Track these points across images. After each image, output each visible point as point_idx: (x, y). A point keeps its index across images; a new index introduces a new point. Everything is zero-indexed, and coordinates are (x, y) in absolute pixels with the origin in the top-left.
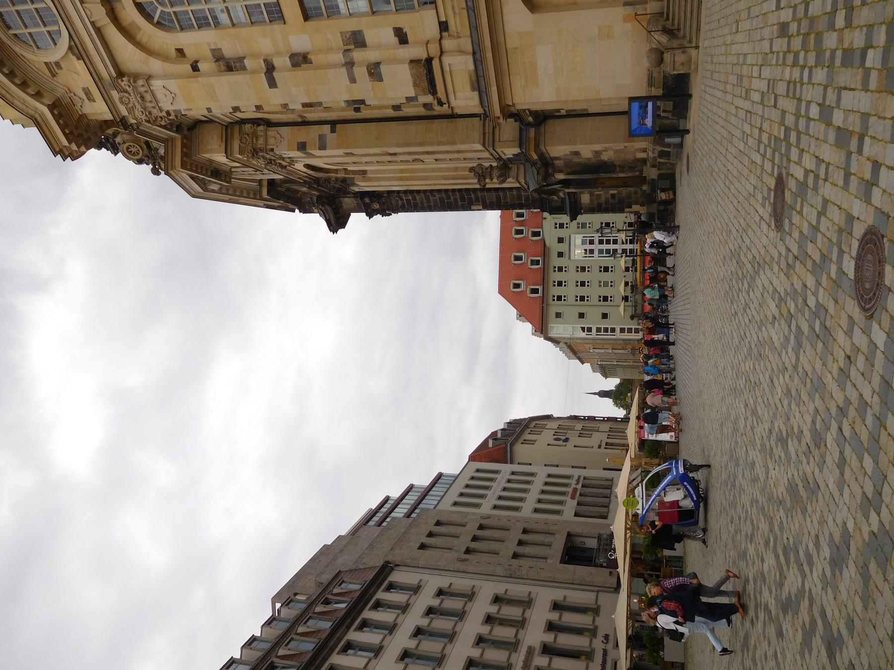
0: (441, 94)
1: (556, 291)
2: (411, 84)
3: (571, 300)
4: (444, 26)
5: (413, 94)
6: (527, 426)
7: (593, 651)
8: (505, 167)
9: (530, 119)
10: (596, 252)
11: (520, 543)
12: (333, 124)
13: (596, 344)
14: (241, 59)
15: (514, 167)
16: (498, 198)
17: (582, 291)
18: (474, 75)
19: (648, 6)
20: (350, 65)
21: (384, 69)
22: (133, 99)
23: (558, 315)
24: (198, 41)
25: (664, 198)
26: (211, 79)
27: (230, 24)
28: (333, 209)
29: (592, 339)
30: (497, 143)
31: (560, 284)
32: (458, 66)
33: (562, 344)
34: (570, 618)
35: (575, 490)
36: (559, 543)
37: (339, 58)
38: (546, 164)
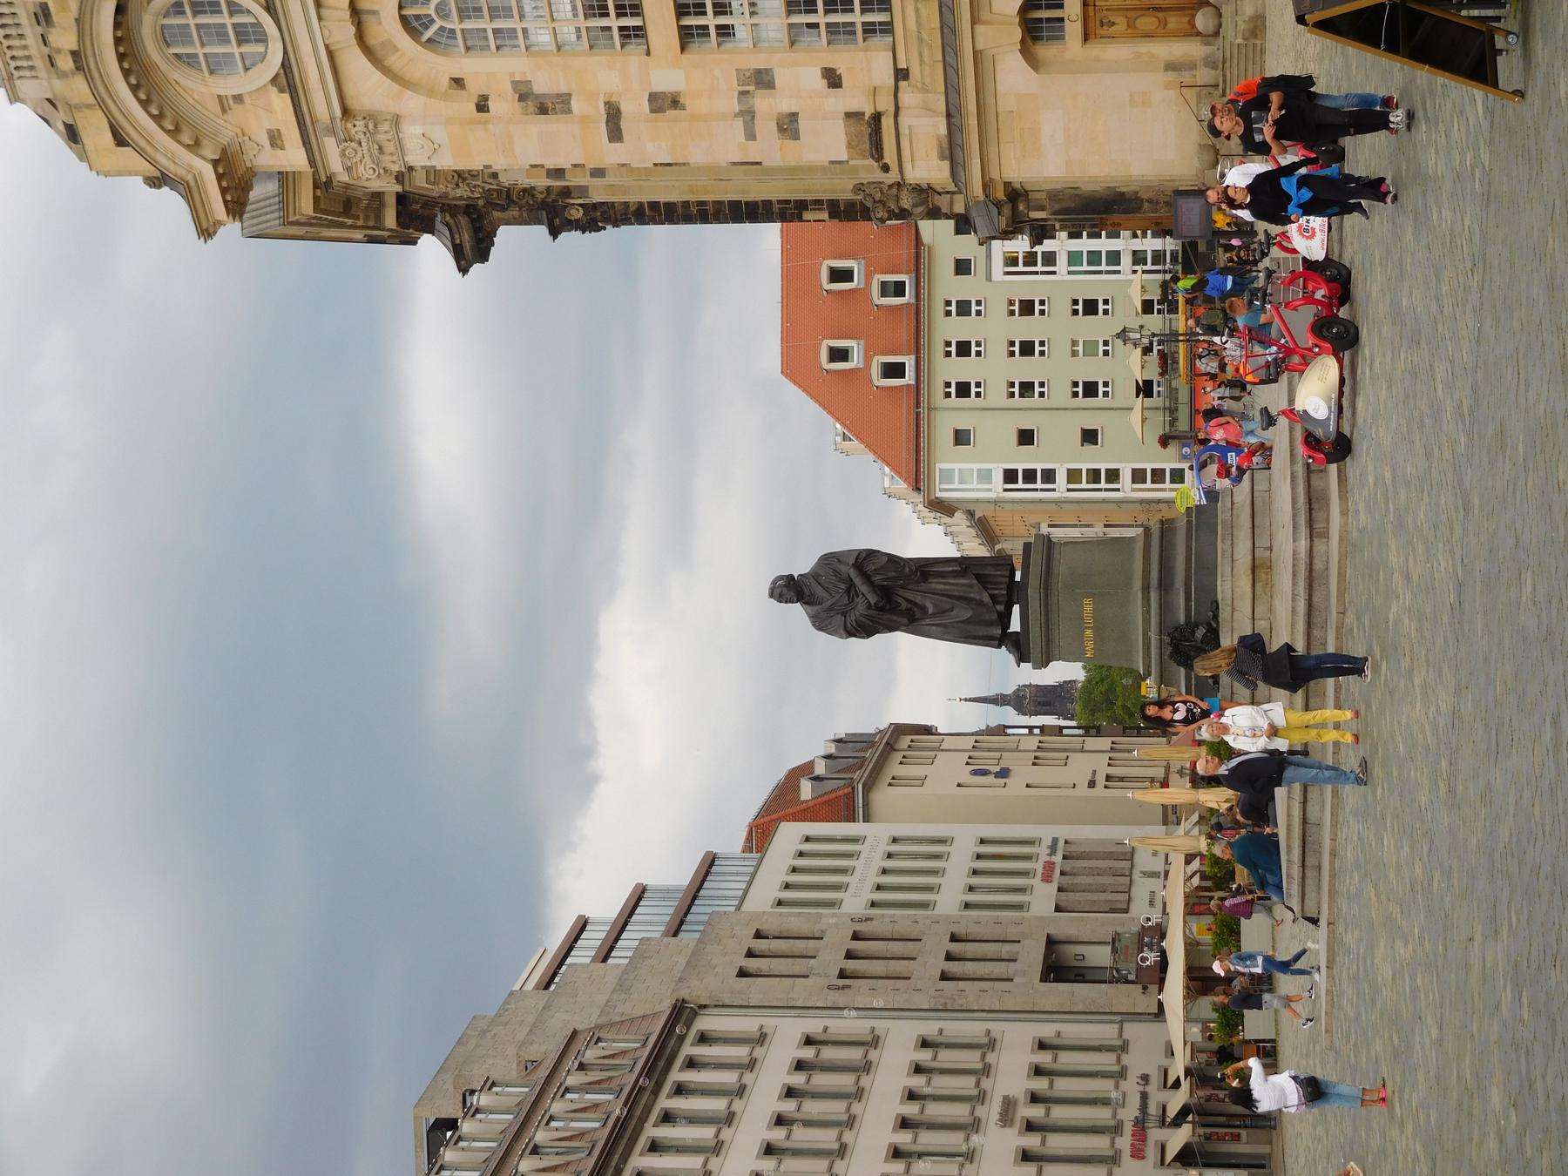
0: (890, 156)
1: (955, 369)
3: (996, 393)
4: (901, 74)
5: (845, 158)
6: (890, 747)
11: (949, 957)
17: (1026, 369)
19: (1197, 73)
20: (748, 115)
21: (803, 124)
23: (961, 438)
24: (491, 70)
28: (473, 221)
29: (1057, 502)
31: (964, 349)
33: (959, 516)
35: (1049, 866)
36: (1033, 955)
37: (734, 105)
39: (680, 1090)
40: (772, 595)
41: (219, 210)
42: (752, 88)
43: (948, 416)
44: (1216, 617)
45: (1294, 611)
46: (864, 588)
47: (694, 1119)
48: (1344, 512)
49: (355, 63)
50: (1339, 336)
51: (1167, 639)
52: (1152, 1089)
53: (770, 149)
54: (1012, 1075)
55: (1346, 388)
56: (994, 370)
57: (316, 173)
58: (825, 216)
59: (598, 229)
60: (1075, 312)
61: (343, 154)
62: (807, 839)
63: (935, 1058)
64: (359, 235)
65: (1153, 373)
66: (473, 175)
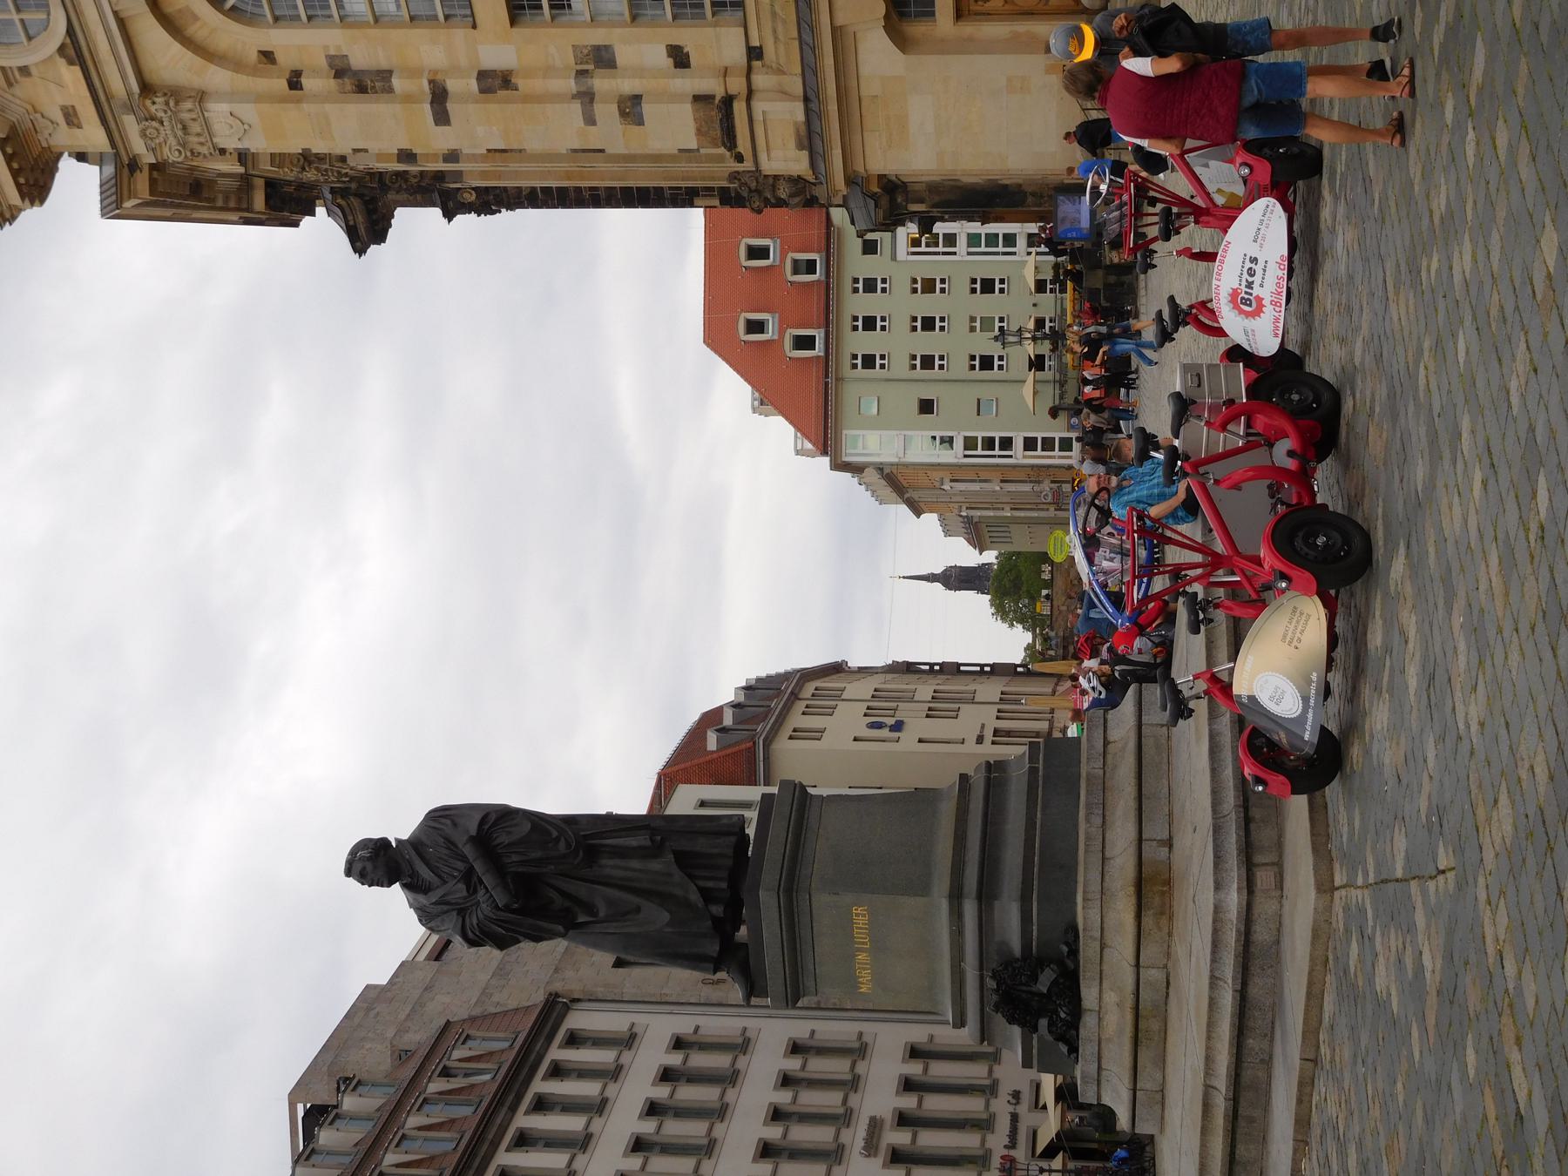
0: (743, 145)
1: (862, 343)
4: (754, 53)
5: (694, 145)
6: (795, 696)
7: (992, 1117)
10: (962, 242)
13: (955, 472)
18: (803, 129)
20: (587, 98)
21: (647, 108)
24: (304, 44)
25: (1116, 260)
26: (328, 107)
27: (371, 19)
28: (366, 203)
31: (869, 324)
33: (870, 474)
37: (570, 85)
39: (557, 1071)
40: (348, 873)
41: (13, 196)
42: (591, 67)
44: (1074, 953)
45: (1214, 980)
46: (488, 880)
47: (584, 1073)
48: (1326, 887)
49: (152, 35)
50: (1332, 555)
51: (991, 984)
52: (1023, 1109)
53: (610, 133)
54: (880, 1097)
55: (1347, 656)
56: (898, 343)
57: (117, 155)
58: (716, 202)
59: (493, 213)
60: (973, 291)
61: (143, 134)
63: (804, 1067)
64: (235, 217)
66: (320, 158)
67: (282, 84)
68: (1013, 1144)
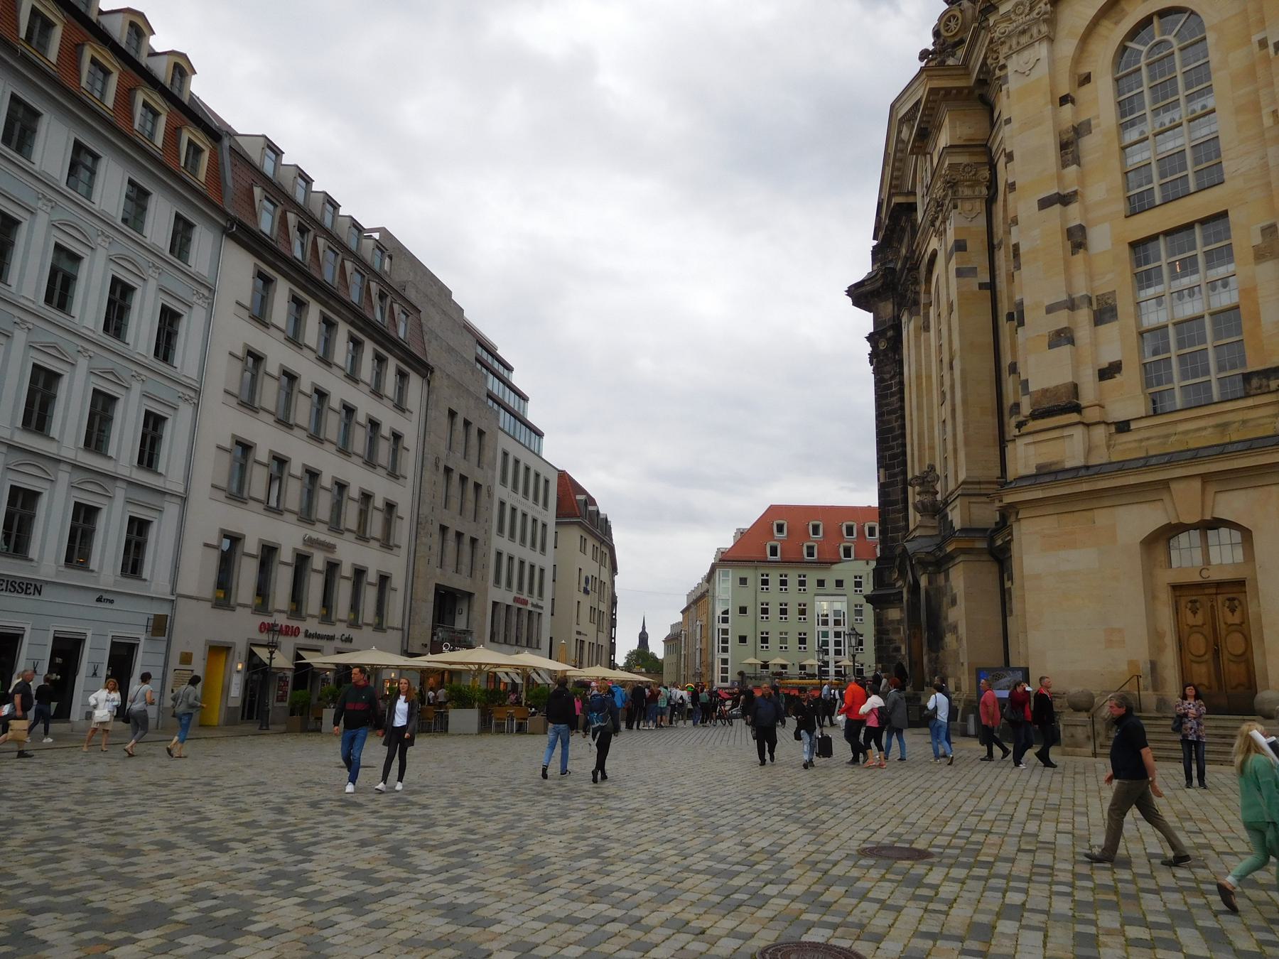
1: (774, 579)
2: (1046, 386)
3: (763, 597)
4: (1123, 427)
5: (1032, 388)
6: (602, 542)
7: (332, 623)
8: (936, 510)
9: (999, 542)
10: (824, 628)
11: (459, 535)
12: (991, 286)
14: (1077, 161)
15: (935, 523)
16: (895, 503)
18: (1058, 467)
19: (1150, 692)
20: (1071, 305)
21: (1066, 349)
22: (1021, 19)
23: (743, 581)
24: (1101, 100)
26: (1049, 125)
30: (966, 499)
31: (783, 583)
32: (1070, 447)
33: (706, 586)
34: (370, 595)
35: (525, 602)
36: (459, 582)
37: (1081, 290)
38: (939, 563)
43: (753, 577)
56: (774, 597)
62: (547, 482)
65: (772, 669)
67: (1064, 90)
68: (308, 635)
